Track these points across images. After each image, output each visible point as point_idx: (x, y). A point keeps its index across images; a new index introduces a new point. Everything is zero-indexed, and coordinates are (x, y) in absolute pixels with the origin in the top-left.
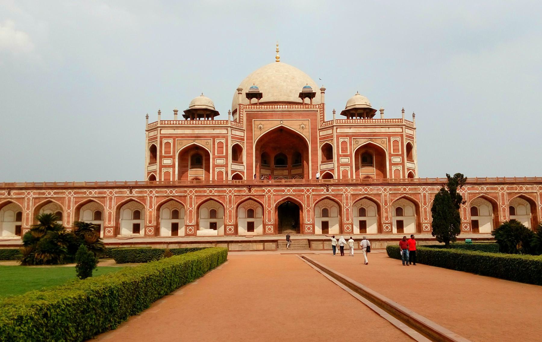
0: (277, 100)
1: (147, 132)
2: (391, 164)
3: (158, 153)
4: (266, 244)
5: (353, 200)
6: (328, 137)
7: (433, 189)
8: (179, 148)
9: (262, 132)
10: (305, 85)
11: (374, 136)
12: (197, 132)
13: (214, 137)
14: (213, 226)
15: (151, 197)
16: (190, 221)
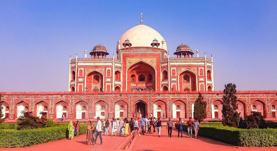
0: (139, 46)
1: (70, 64)
2: (199, 82)
7: (213, 96)
10: (154, 39)
11: (189, 66)
13: (105, 67)
14: (103, 114)
15: (72, 100)
16: (91, 112)
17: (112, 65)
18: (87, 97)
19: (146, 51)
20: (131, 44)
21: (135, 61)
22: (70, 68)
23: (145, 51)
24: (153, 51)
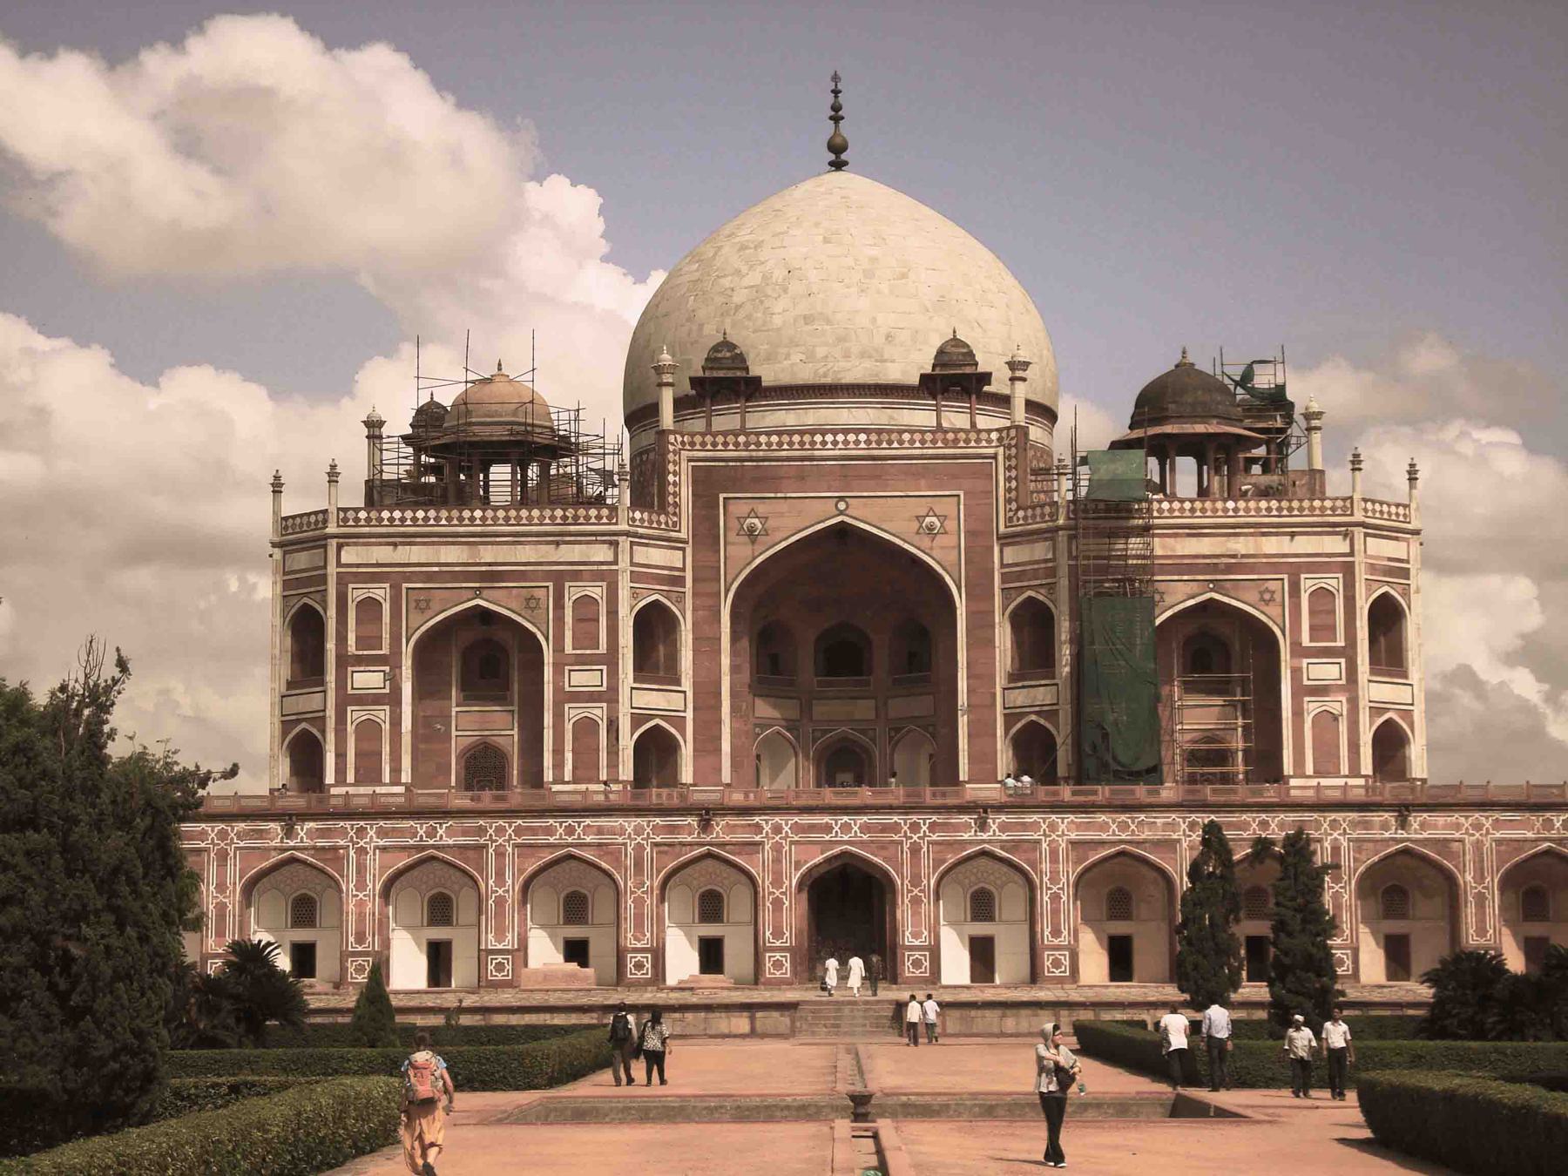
0: (828, 380)
1: (278, 553)
2: (1300, 691)
3: (331, 645)
4: (759, 1015)
5: (1077, 863)
6: (1035, 574)
7: (1367, 825)
8: (414, 625)
9: (759, 548)
11: (1229, 569)
12: (488, 554)
13: (560, 579)
14: (576, 951)
15: (362, 851)
16: (500, 934)
17: (610, 558)
18: (465, 833)
19: (879, 442)
20: (758, 379)
21: (794, 518)
22: (279, 579)
23: (874, 437)
24: (939, 436)
